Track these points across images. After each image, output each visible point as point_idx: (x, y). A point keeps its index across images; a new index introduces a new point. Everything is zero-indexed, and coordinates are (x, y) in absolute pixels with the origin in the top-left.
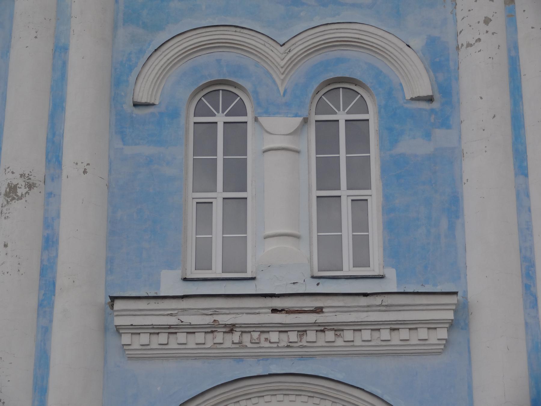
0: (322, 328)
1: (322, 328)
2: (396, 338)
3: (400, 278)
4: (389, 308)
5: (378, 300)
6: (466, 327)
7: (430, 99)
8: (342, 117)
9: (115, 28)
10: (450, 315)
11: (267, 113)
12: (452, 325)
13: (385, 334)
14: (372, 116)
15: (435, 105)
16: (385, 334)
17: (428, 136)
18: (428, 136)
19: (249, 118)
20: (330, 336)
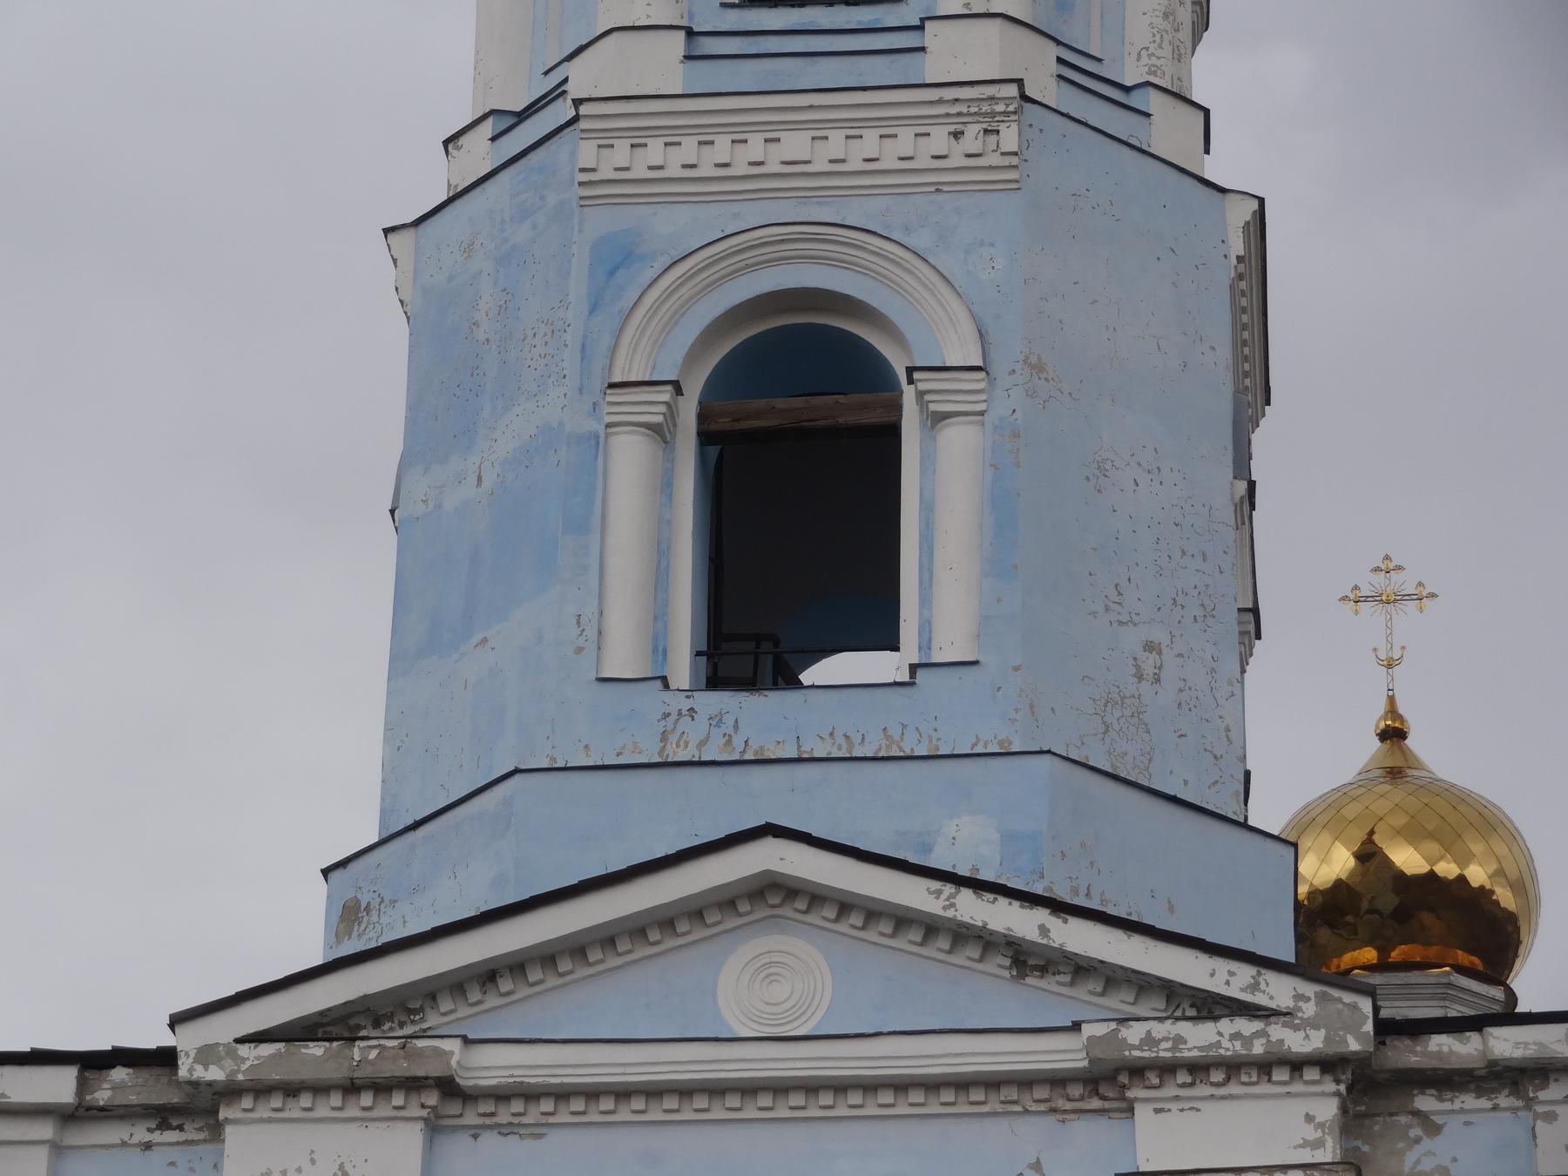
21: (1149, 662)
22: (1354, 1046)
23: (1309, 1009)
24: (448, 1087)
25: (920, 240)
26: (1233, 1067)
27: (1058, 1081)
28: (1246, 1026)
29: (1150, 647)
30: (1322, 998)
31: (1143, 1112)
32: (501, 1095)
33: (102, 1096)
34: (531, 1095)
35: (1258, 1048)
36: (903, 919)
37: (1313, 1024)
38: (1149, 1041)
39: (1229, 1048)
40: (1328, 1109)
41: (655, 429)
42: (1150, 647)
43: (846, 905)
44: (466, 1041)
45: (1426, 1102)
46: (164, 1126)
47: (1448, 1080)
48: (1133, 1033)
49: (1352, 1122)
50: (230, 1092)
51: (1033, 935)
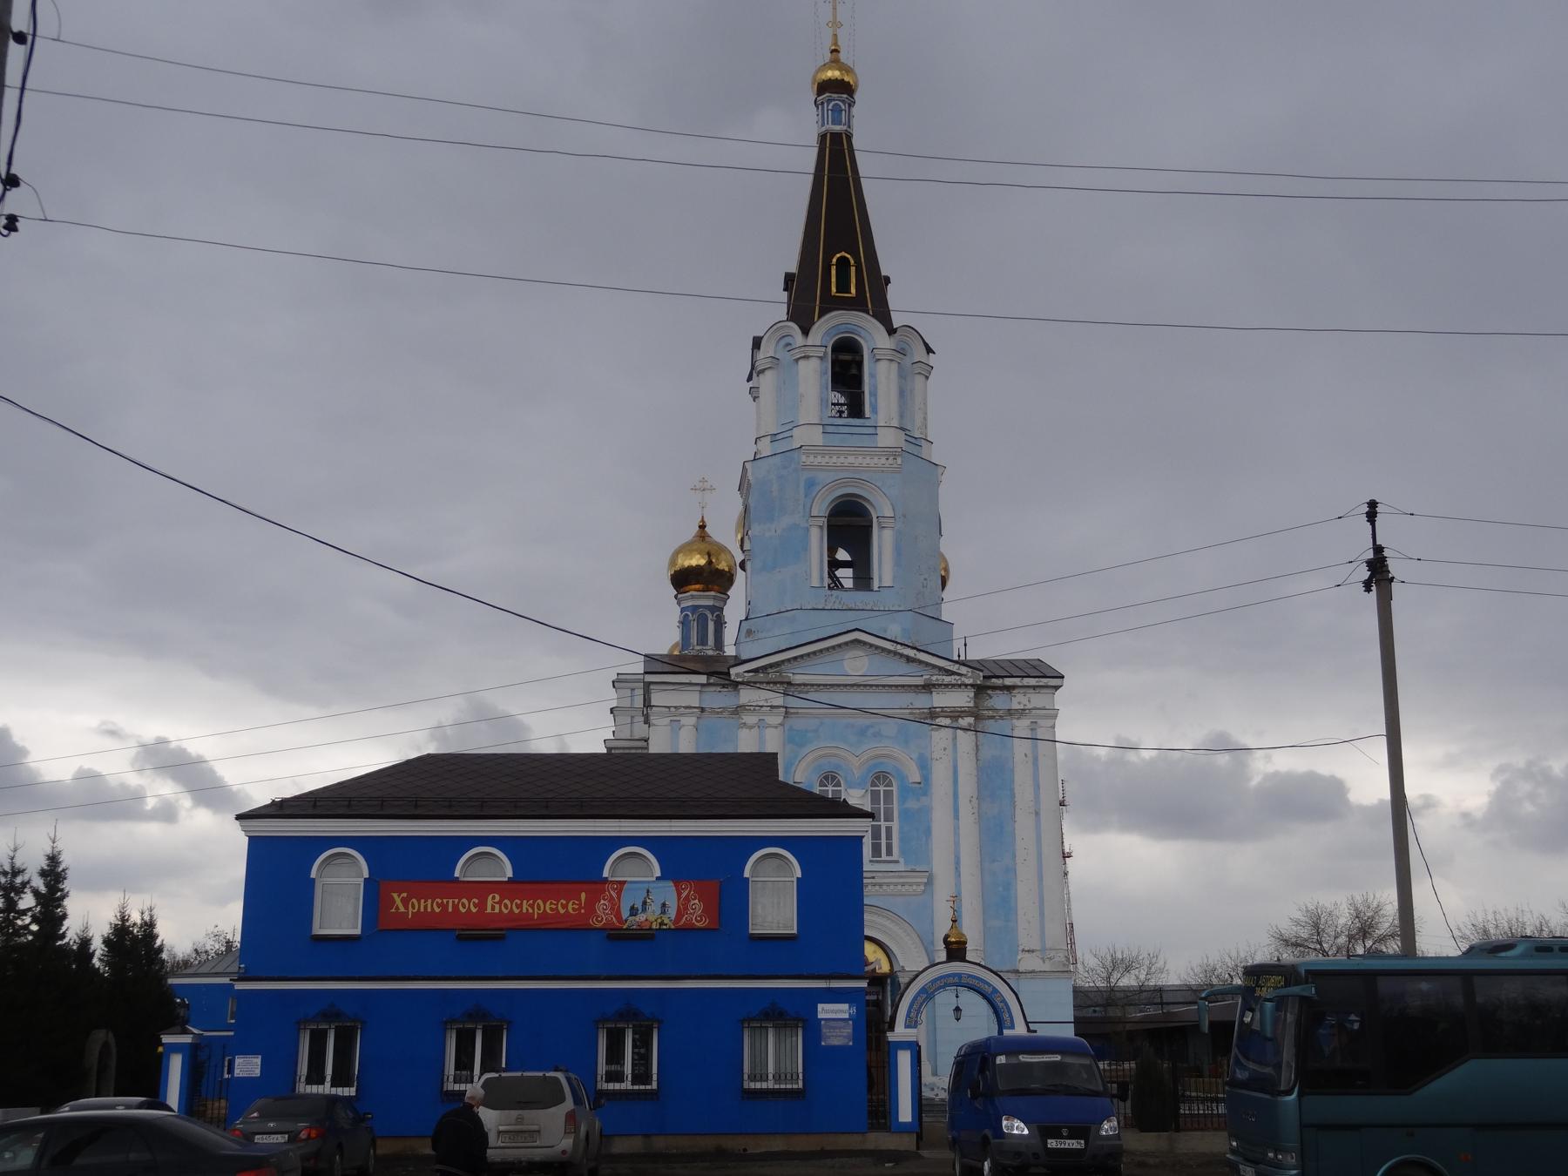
0: (874, 885)
1: (874, 885)
2: (903, 889)
3: (906, 864)
4: (901, 877)
5: (897, 874)
6: (932, 884)
7: (920, 783)
8: (882, 788)
9: (784, 745)
10: (926, 880)
11: (851, 787)
12: (926, 884)
13: (899, 887)
14: (894, 789)
15: (922, 785)
16: (899, 887)
17: (918, 800)
18: (918, 800)
19: (842, 788)
20: (877, 888)
21: (925, 582)
22: (979, 682)
23: (970, 674)
24: (789, 683)
25: (879, 484)
26: (953, 685)
27: (917, 686)
28: (958, 678)
29: (925, 579)
30: (972, 672)
31: (934, 694)
32: (799, 685)
33: (712, 681)
34: (805, 685)
35: (959, 683)
36: (883, 650)
37: (970, 677)
38: (937, 680)
39: (954, 682)
40: (972, 695)
41: (820, 526)
42: (925, 579)
43: (871, 645)
44: (793, 674)
45: (990, 692)
46: (724, 687)
47: (994, 688)
48: (934, 678)
49: (976, 695)
50: (742, 683)
51: (913, 655)
